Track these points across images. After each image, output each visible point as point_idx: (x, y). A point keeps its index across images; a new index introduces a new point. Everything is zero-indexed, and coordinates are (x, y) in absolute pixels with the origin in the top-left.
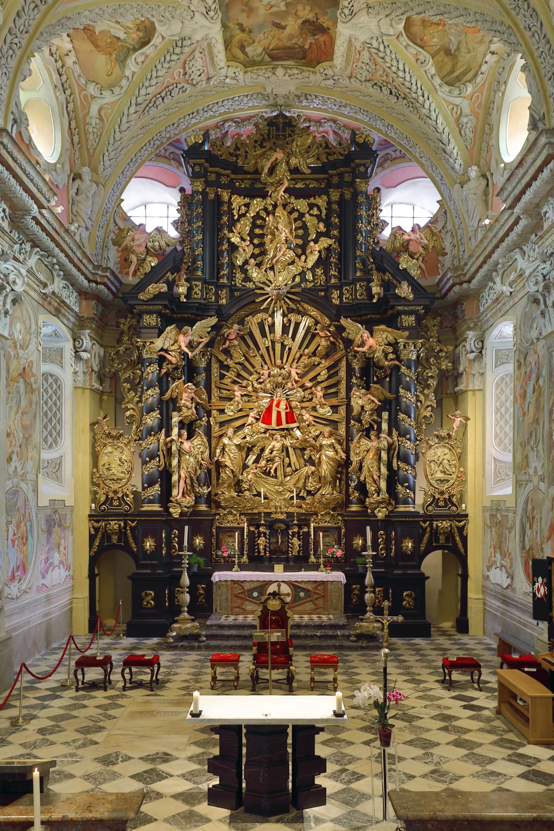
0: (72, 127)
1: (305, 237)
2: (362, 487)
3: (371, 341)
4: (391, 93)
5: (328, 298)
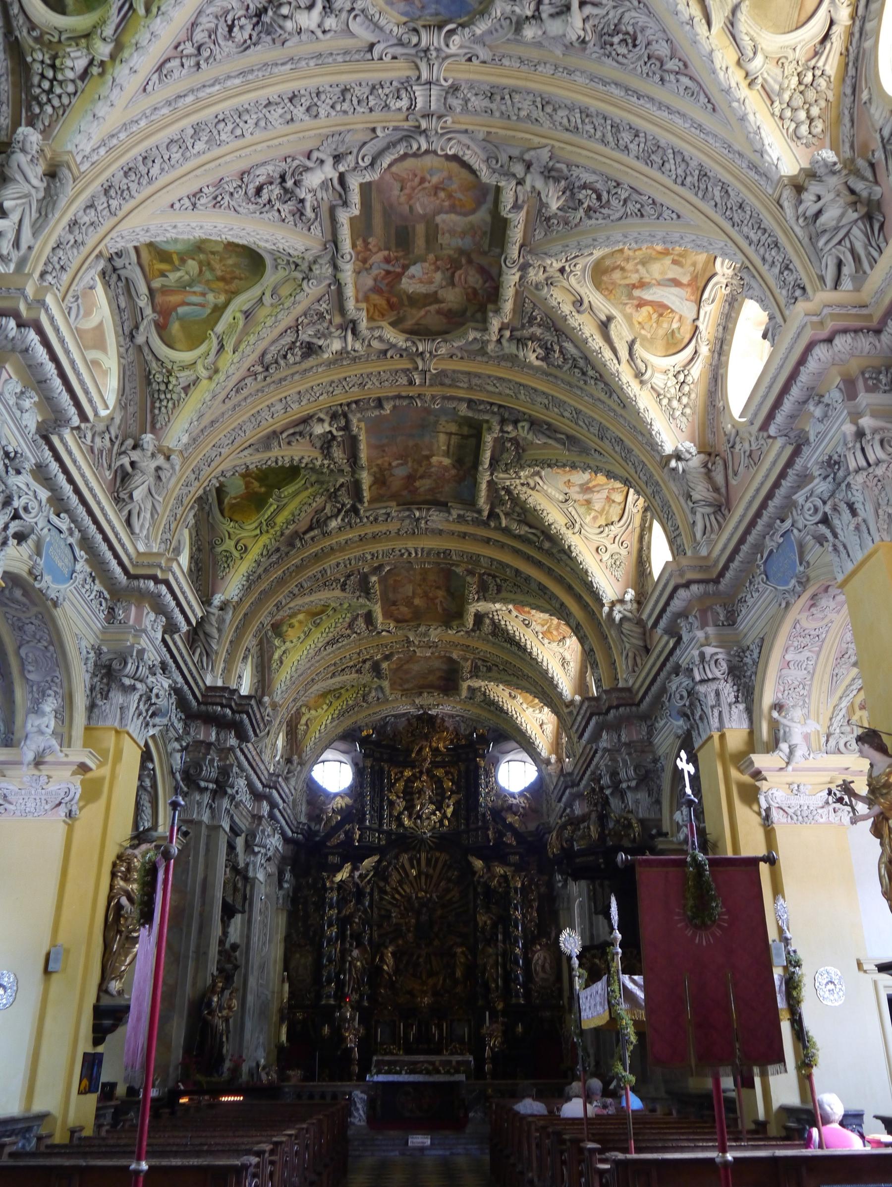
2: (486, 986)
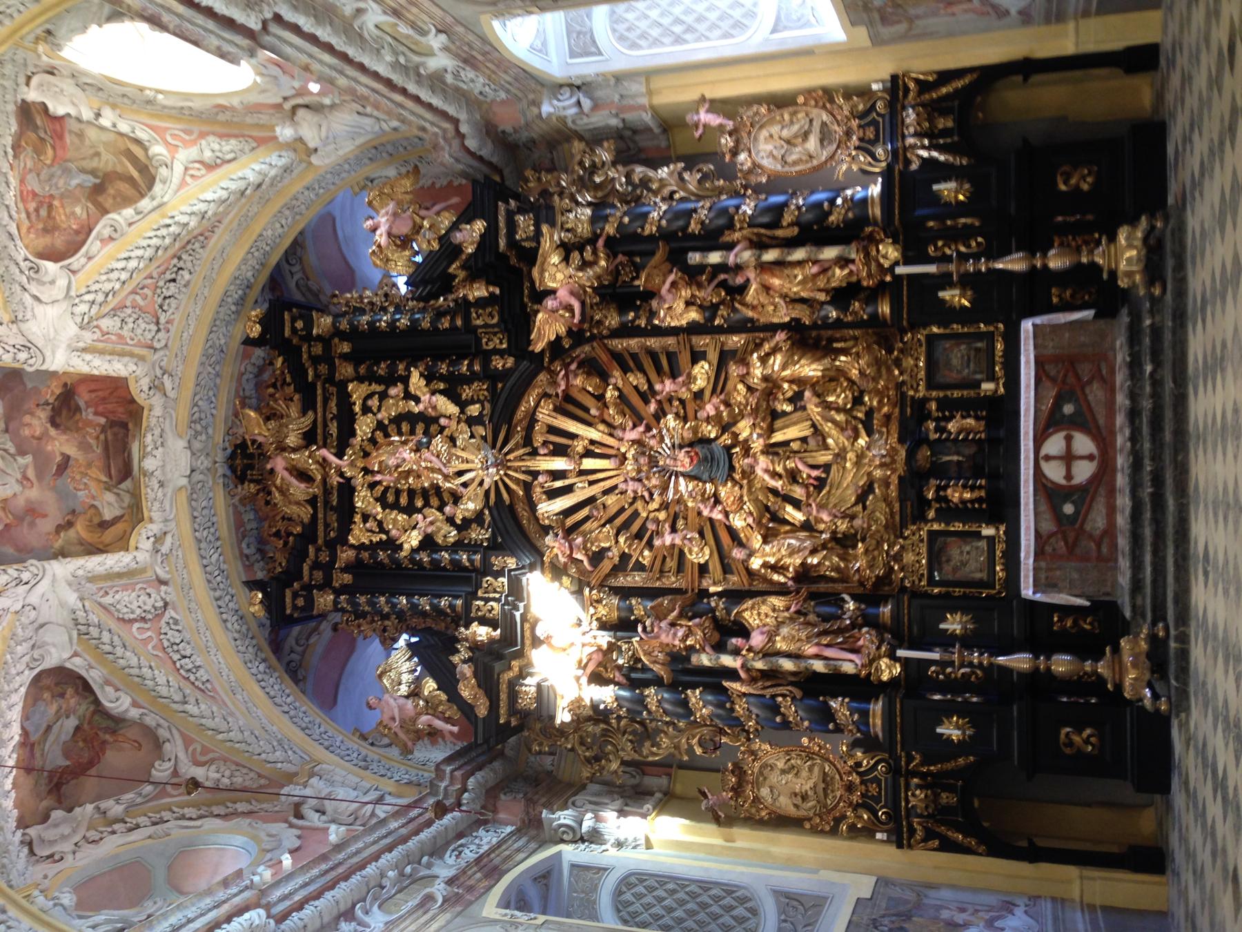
0: (222, 813)
1: (412, 418)
2: (841, 296)
4: (174, 280)
5: (505, 374)
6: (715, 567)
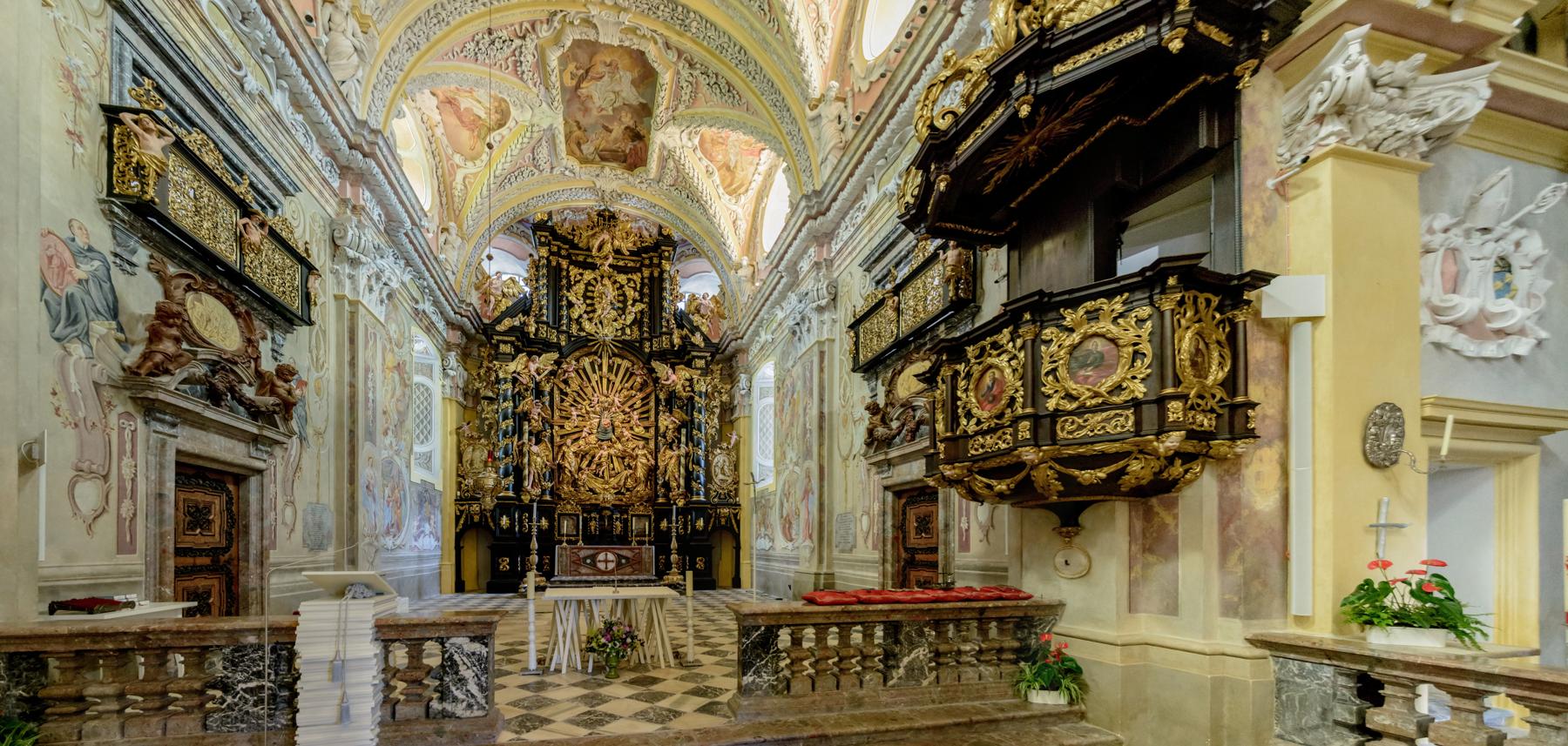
1: (624, 302)
2: (666, 485)
3: (674, 377)
6: (563, 432)
